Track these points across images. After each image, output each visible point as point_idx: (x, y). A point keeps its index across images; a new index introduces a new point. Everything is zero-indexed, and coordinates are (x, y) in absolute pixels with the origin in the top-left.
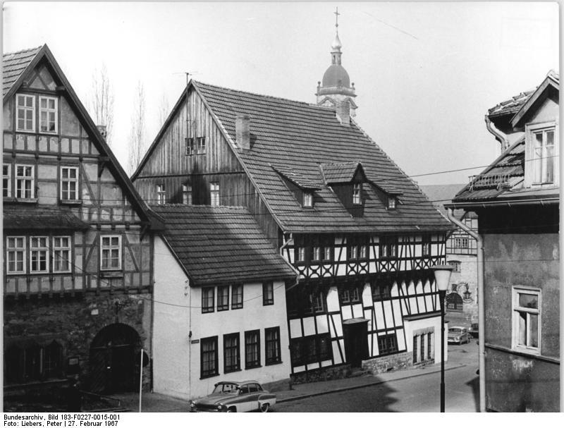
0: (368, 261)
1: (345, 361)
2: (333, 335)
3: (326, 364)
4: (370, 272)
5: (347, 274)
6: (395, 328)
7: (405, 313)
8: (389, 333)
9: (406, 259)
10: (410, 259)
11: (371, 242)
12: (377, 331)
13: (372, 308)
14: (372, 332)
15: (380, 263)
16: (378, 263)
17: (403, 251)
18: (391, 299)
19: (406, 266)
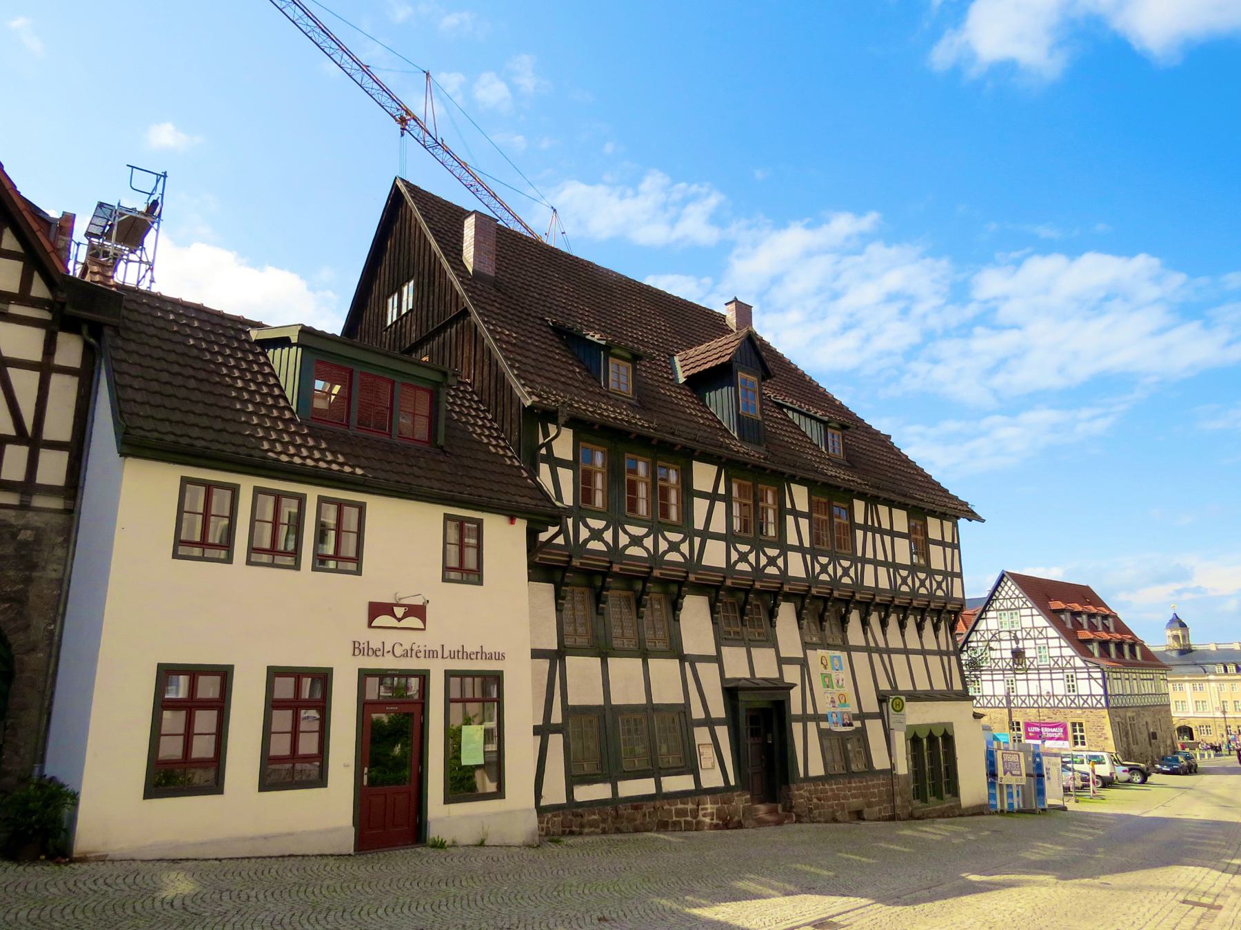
0: (785, 548)
1: (732, 783)
2: (697, 713)
3: (683, 783)
9: (876, 563)
10: (885, 564)
12: (818, 718)
13: (803, 663)
14: (804, 718)
15: (814, 558)
16: (808, 557)
19: (875, 579)
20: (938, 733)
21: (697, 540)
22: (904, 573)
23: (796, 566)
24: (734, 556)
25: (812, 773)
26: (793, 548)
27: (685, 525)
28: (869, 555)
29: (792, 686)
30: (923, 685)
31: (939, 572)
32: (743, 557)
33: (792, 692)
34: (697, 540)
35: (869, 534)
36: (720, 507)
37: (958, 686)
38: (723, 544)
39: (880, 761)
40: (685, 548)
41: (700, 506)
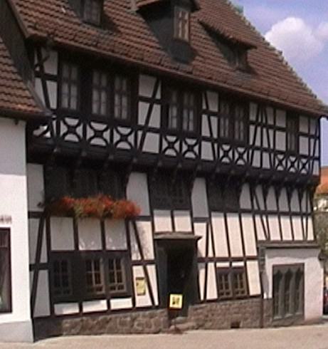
0: (200, 139)
2: (135, 256)
3: (126, 303)
4: (203, 157)
5: (162, 151)
6: (245, 259)
7: (262, 237)
8: (234, 264)
9: (262, 150)
11: (204, 107)
12: (215, 260)
13: (208, 221)
14: (206, 261)
16: (216, 146)
17: (257, 136)
18: (240, 212)
19: (261, 161)
20: (294, 270)
21: (140, 133)
22: (281, 157)
23: (207, 152)
24: (165, 145)
25: (208, 297)
26: (206, 139)
27: (132, 122)
28: (258, 143)
29: (200, 238)
30: (287, 237)
31: (304, 157)
32: (171, 145)
33: (199, 242)
34: (140, 133)
35: (259, 129)
36: (157, 109)
37: (311, 237)
38: (157, 136)
39: (254, 289)
40: (131, 139)
41: (143, 108)
